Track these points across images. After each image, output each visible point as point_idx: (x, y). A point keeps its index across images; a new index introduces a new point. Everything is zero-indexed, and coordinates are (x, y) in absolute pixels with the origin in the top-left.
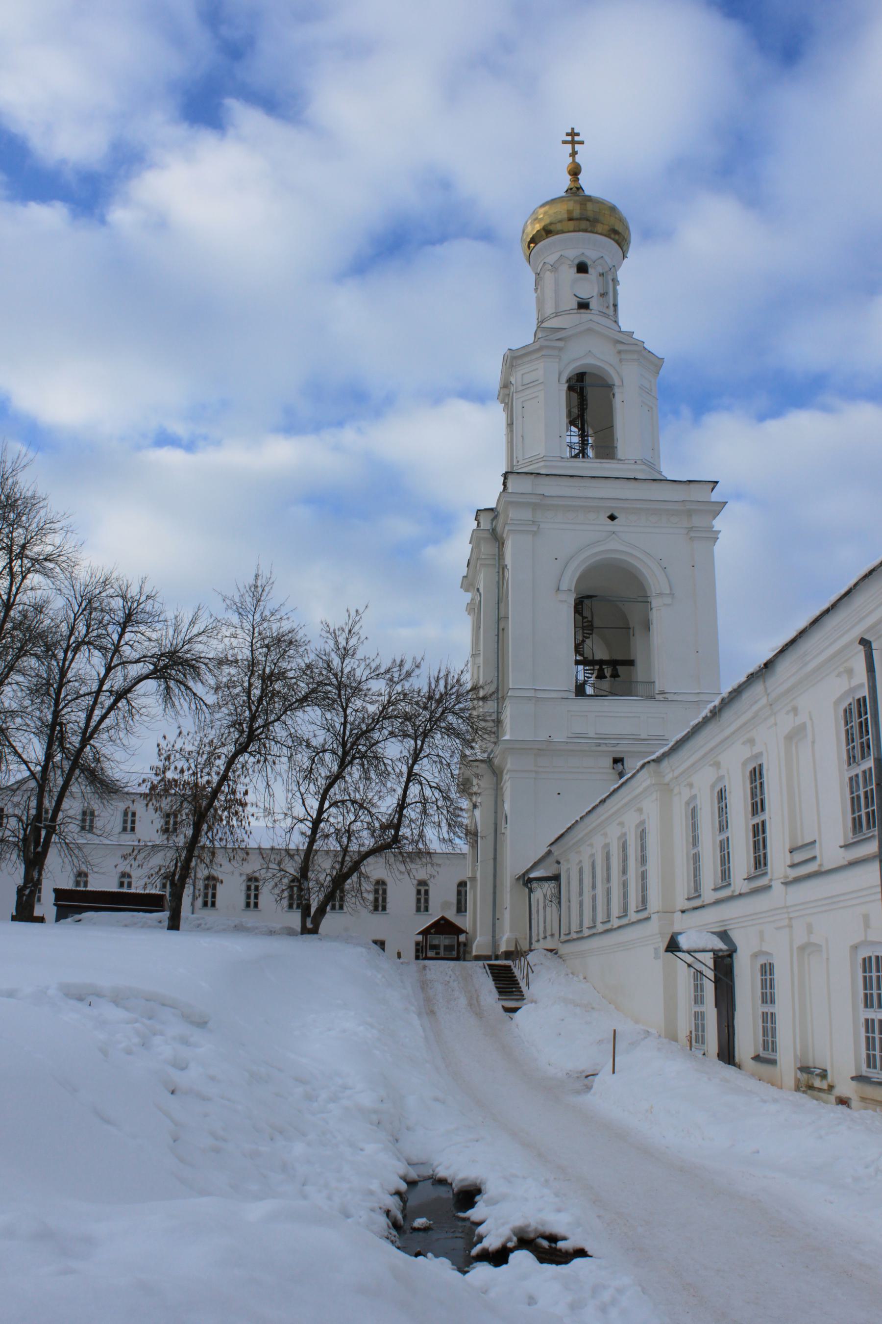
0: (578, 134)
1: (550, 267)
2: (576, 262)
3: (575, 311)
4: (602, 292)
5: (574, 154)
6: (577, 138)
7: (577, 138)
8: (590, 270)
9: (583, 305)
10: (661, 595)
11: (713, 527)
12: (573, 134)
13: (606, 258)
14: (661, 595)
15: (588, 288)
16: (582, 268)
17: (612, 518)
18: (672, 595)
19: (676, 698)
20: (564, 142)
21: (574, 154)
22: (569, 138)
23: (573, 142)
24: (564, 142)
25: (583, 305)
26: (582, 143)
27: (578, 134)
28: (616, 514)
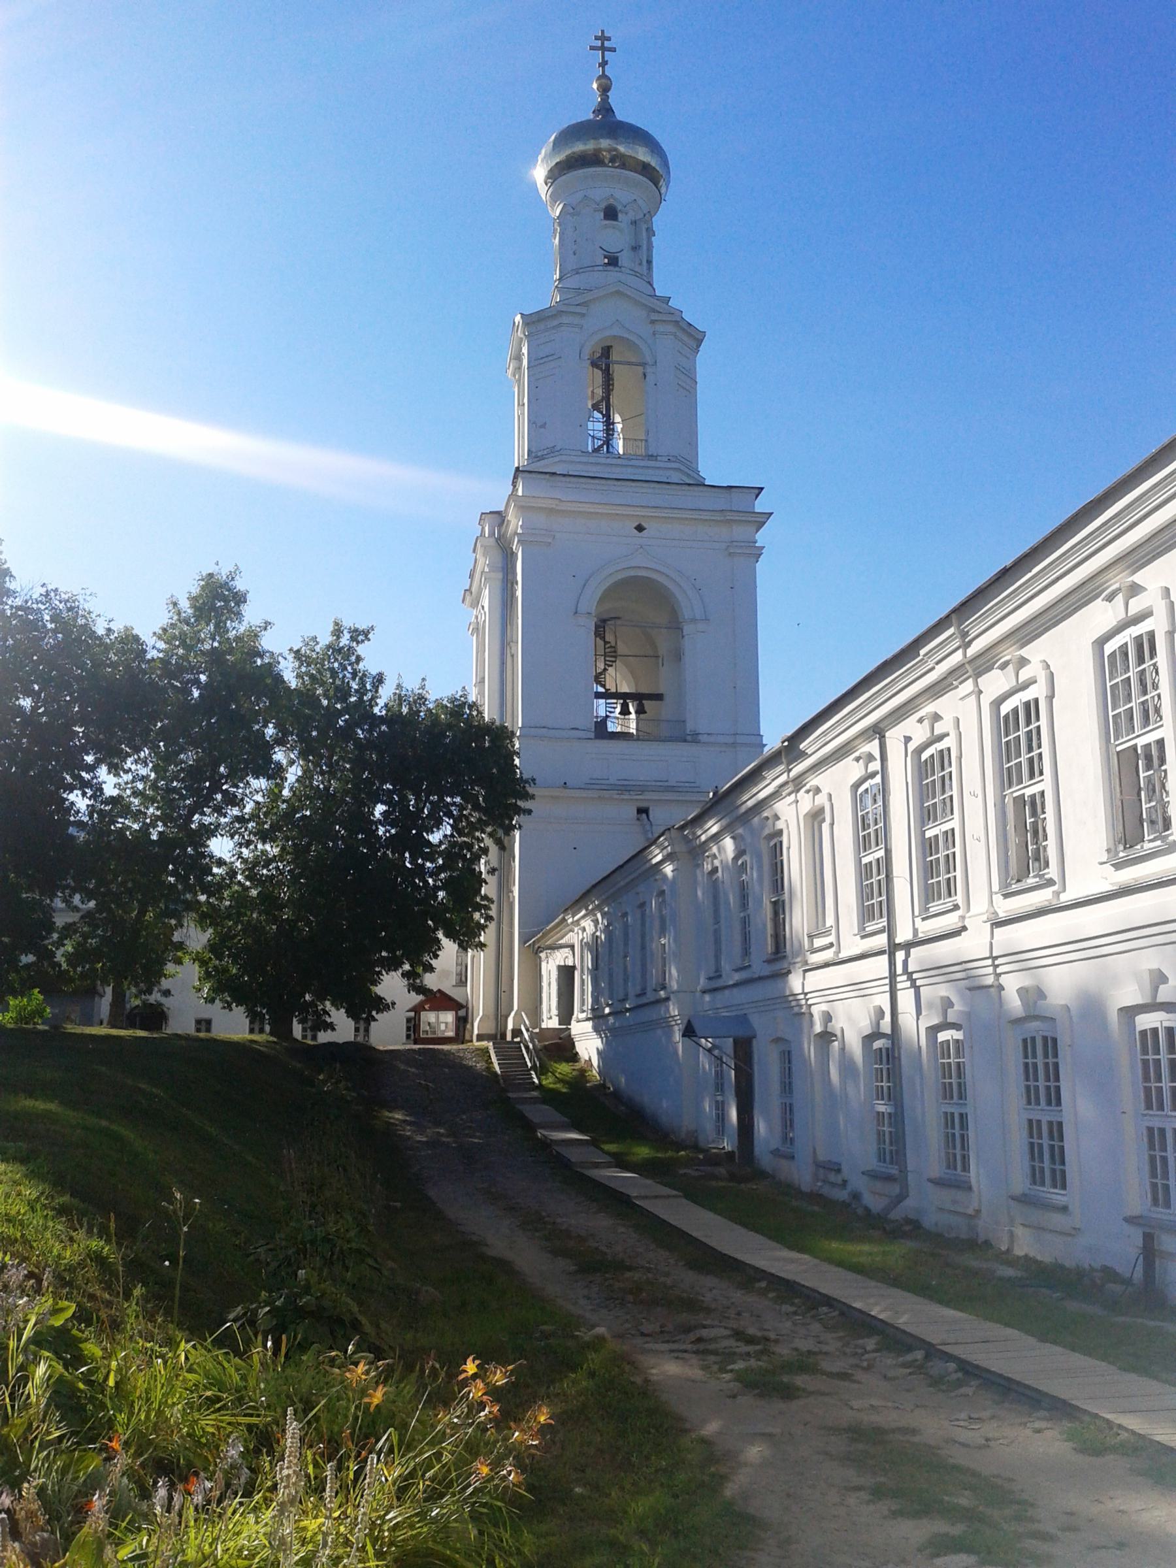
0: (609, 39)
1: (572, 211)
2: (603, 205)
4: (633, 244)
5: (604, 64)
6: (607, 44)
7: (607, 44)
10: (694, 620)
11: (756, 542)
12: (603, 38)
14: (694, 620)
15: (615, 238)
16: (611, 213)
17: (640, 528)
19: (712, 739)
20: (592, 48)
21: (604, 64)
22: (599, 43)
23: (603, 49)
24: (592, 48)
26: (613, 50)
27: (609, 39)
28: (644, 524)
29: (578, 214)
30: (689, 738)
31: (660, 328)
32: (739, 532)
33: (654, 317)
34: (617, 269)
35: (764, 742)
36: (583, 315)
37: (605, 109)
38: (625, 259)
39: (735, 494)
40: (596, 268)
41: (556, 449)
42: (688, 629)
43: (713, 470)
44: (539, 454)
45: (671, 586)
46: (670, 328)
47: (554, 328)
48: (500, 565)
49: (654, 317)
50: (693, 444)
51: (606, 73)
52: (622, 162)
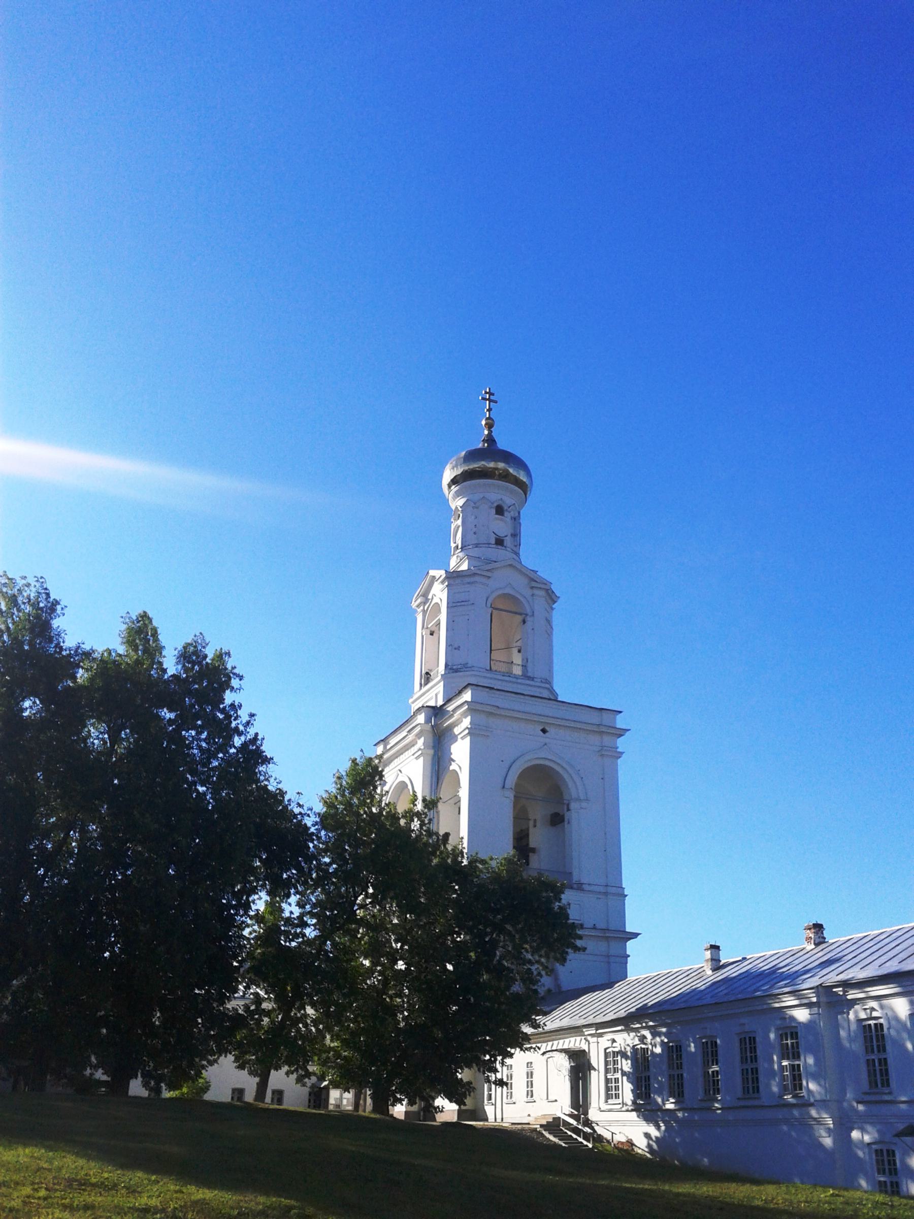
0: (493, 394)
2: (495, 505)
3: (494, 546)
5: (490, 410)
6: (492, 397)
7: (492, 397)
8: (506, 514)
9: (500, 542)
11: (617, 748)
13: (516, 505)
14: (578, 800)
15: (502, 527)
16: (500, 510)
18: (587, 800)
23: (489, 400)
25: (500, 542)
26: (496, 402)
27: (493, 394)
28: (547, 729)
29: (477, 508)
30: (575, 886)
31: (537, 592)
32: (607, 740)
33: (534, 584)
34: (504, 548)
35: (626, 893)
36: (489, 577)
37: (490, 440)
38: (508, 541)
39: (604, 714)
40: (490, 546)
41: (469, 665)
42: (573, 806)
43: (565, 690)
44: (454, 667)
45: (565, 776)
46: (542, 593)
47: (469, 583)
48: (432, 744)
49: (534, 584)
50: (550, 670)
51: (491, 416)
52: (505, 476)
